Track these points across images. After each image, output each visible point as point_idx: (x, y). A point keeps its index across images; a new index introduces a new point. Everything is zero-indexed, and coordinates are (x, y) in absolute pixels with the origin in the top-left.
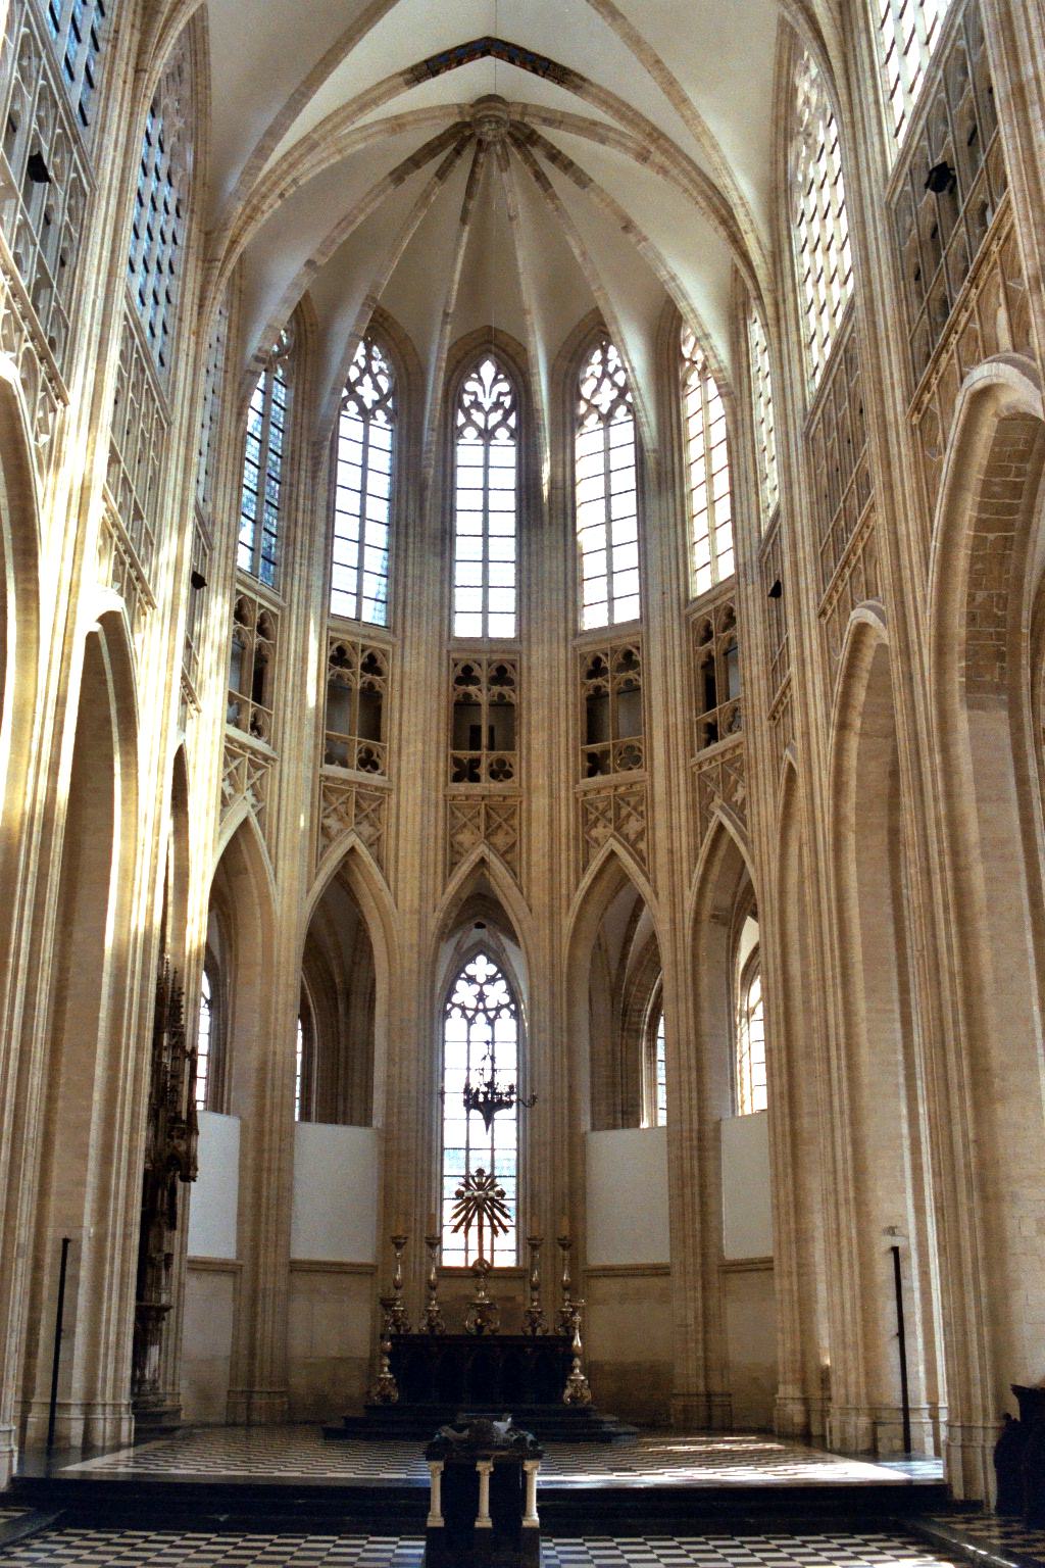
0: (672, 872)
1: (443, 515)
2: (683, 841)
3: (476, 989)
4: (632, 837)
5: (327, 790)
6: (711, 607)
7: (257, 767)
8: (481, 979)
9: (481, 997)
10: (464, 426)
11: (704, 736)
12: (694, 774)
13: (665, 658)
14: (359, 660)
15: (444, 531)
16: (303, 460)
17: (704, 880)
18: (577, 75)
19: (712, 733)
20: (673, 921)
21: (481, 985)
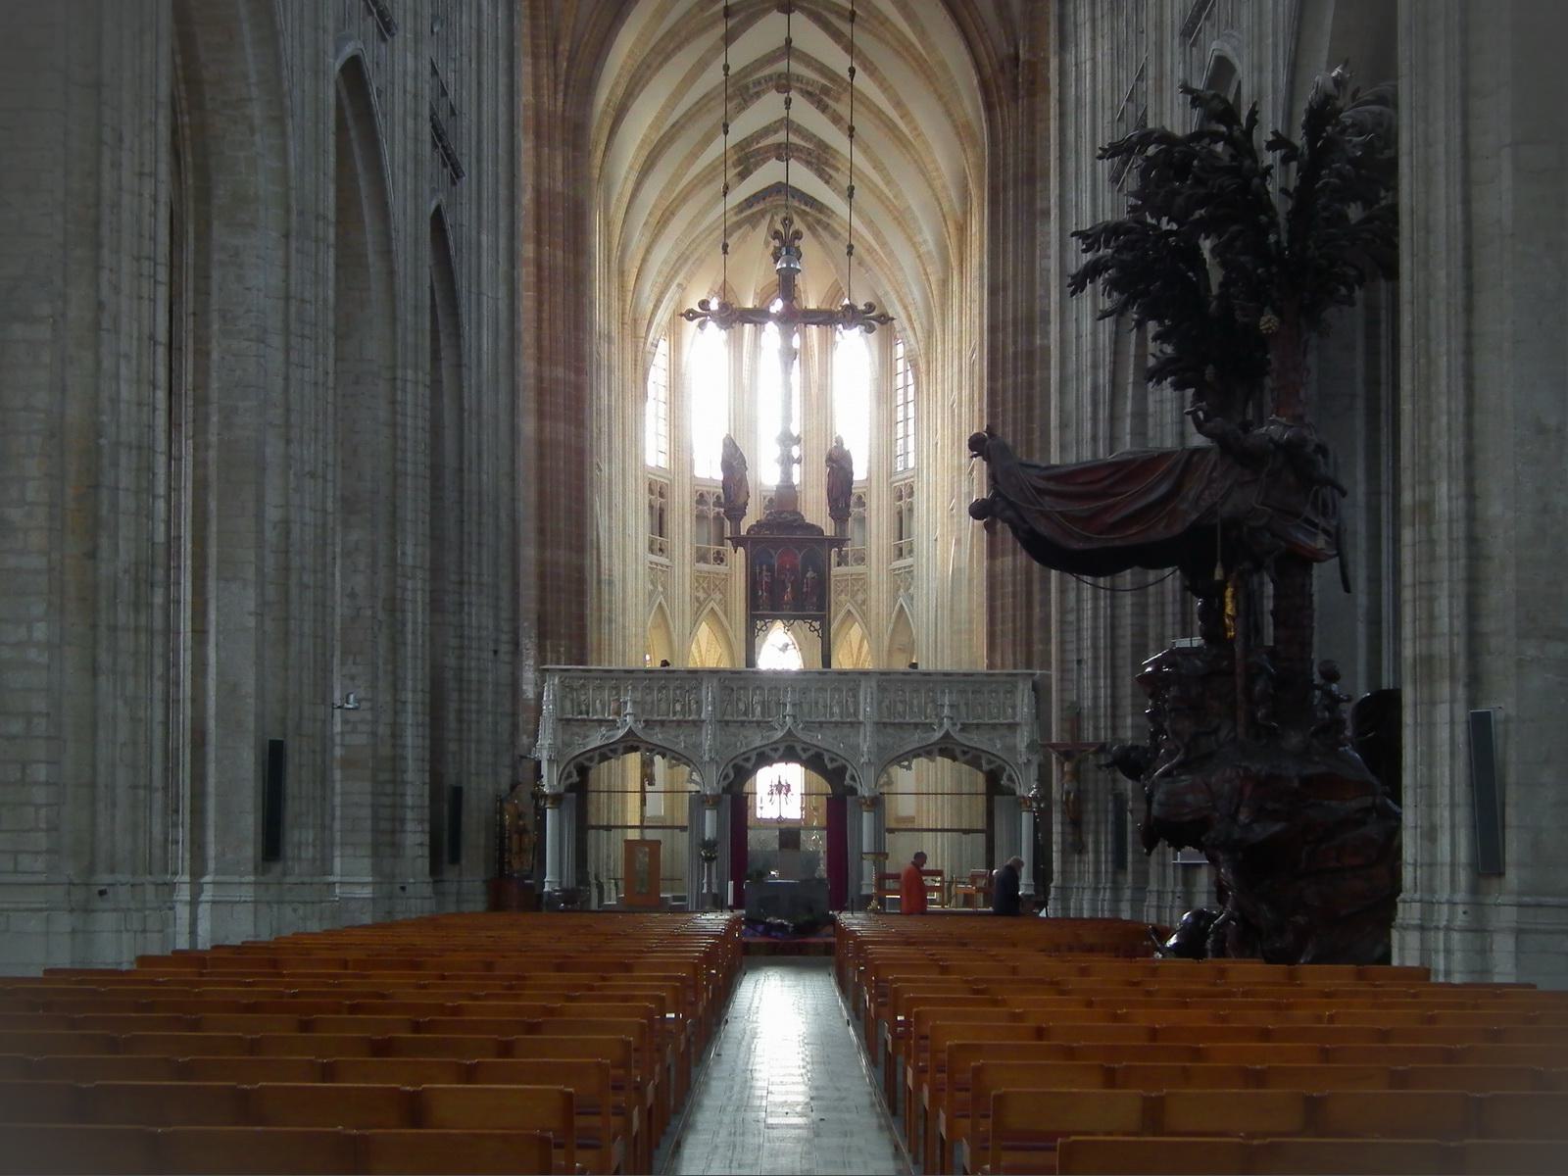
5: (699, 578)
7: (663, 572)
11: (897, 552)
14: (712, 500)
18: (828, 208)
19: (900, 555)
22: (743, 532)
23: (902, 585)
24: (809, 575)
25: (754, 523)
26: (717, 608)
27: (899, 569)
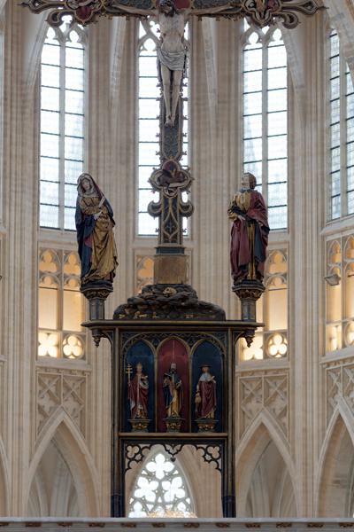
0: (305, 446)
1: (128, 124)
2: (315, 423)
3: (155, 485)
4: (278, 412)
6: (339, 236)
8: (160, 475)
9: (160, 492)
10: (145, 38)
12: (323, 369)
13: (305, 270)
15: (128, 141)
16: (14, 98)
17: (328, 454)
20: (305, 485)
21: (160, 482)
22: (109, 316)
23: (340, 386)
24: (206, 377)
25: (124, 302)
26: (70, 424)
27: (336, 362)
